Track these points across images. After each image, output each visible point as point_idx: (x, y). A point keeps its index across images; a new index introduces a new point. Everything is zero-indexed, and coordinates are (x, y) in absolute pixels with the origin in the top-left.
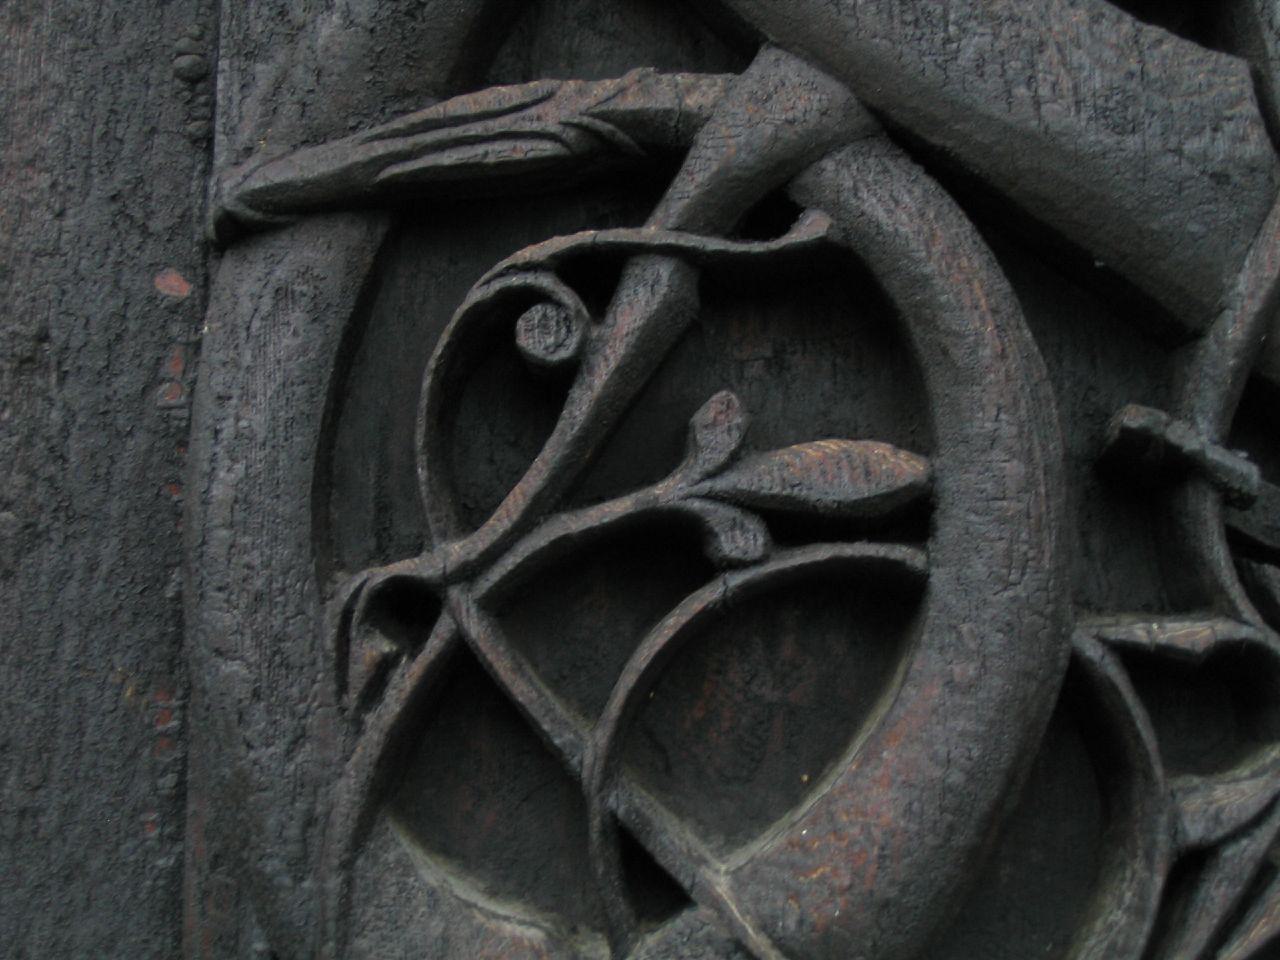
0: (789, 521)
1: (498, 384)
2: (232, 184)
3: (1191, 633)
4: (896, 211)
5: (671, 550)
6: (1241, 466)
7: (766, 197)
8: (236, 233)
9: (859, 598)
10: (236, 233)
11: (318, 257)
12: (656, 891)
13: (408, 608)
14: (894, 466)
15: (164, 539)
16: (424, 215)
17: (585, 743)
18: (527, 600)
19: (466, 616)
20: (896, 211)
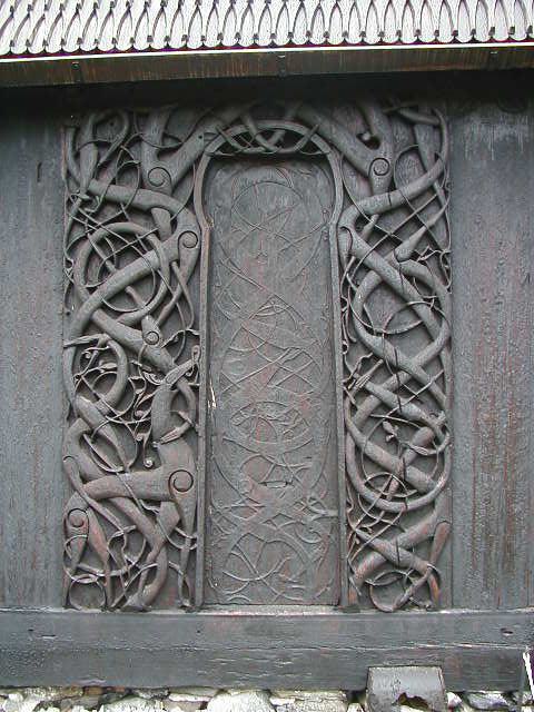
0: (106, 370)
1: (84, 359)
2: (66, 344)
3: (137, 378)
4: (114, 346)
5: (98, 372)
7: (104, 345)
8: (65, 348)
9: (111, 377)
10: (65, 348)
11: (72, 350)
12: (98, 399)
13: (79, 377)
14: (115, 365)
15: (62, 371)
16: (80, 347)
17: (91, 386)
18: (87, 376)
20: (114, 346)
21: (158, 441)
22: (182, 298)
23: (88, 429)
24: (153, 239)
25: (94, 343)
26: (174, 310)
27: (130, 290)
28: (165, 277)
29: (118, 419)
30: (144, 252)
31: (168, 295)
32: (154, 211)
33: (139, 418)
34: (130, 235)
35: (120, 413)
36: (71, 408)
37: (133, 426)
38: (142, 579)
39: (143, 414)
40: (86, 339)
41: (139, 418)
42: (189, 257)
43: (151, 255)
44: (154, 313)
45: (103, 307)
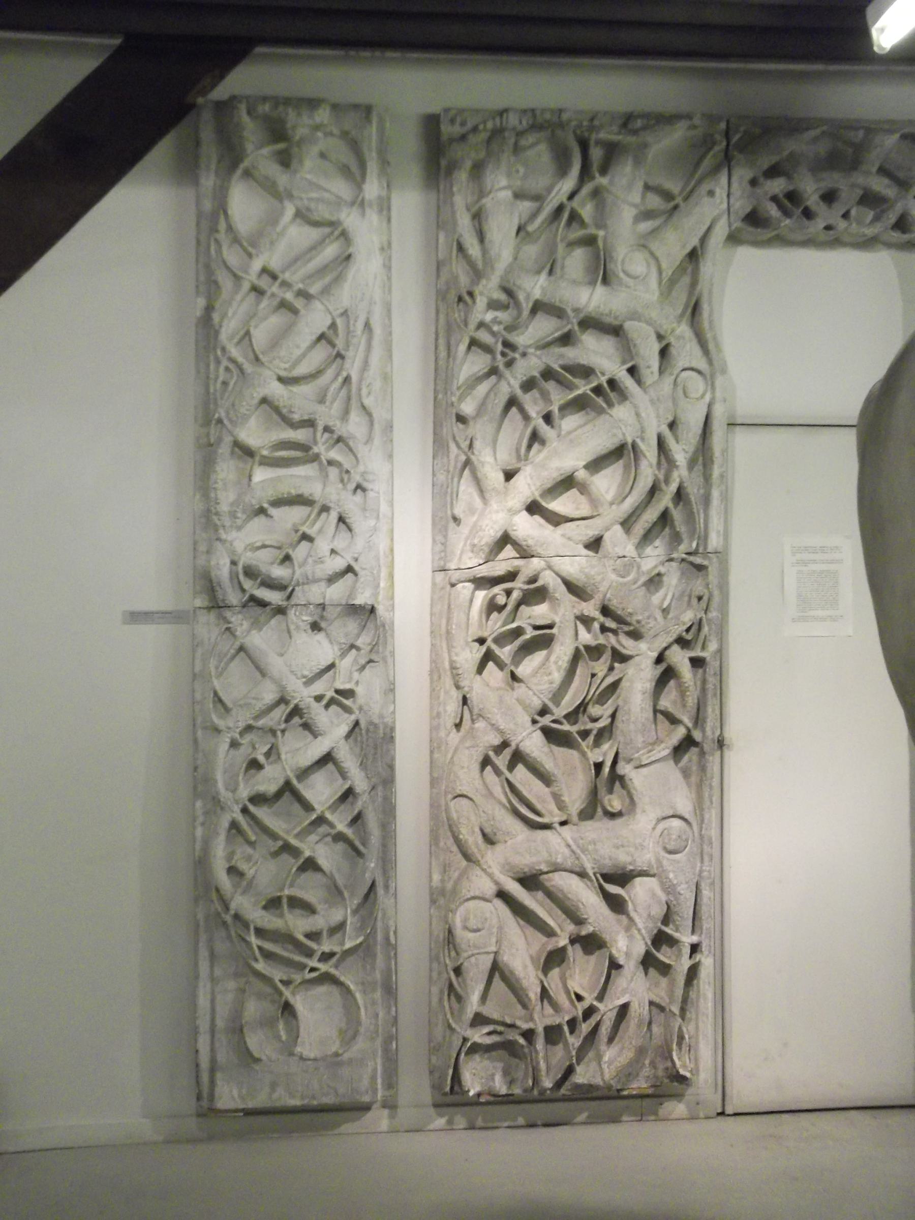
6: (602, 619)
19: (489, 642)
21: (629, 761)
22: (680, 496)
23: (497, 741)
24: (628, 382)
25: (512, 576)
26: (665, 518)
27: (581, 474)
28: (650, 451)
29: (554, 721)
30: (610, 405)
31: (653, 491)
32: (628, 325)
33: (595, 720)
34: (586, 372)
35: (560, 712)
36: (465, 700)
37: (585, 734)
38: (605, 1030)
39: (602, 711)
40: (499, 568)
41: (595, 720)
42: (693, 419)
43: (621, 412)
44: (627, 523)
45: (533, 508)
